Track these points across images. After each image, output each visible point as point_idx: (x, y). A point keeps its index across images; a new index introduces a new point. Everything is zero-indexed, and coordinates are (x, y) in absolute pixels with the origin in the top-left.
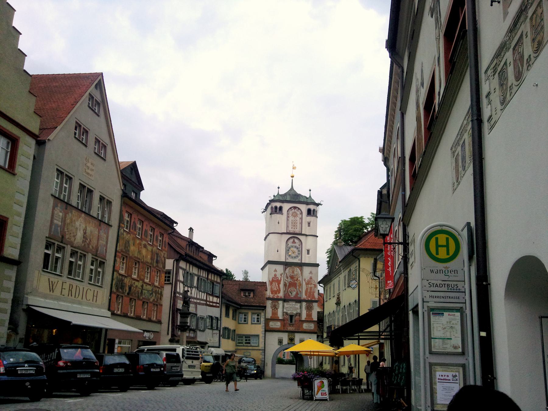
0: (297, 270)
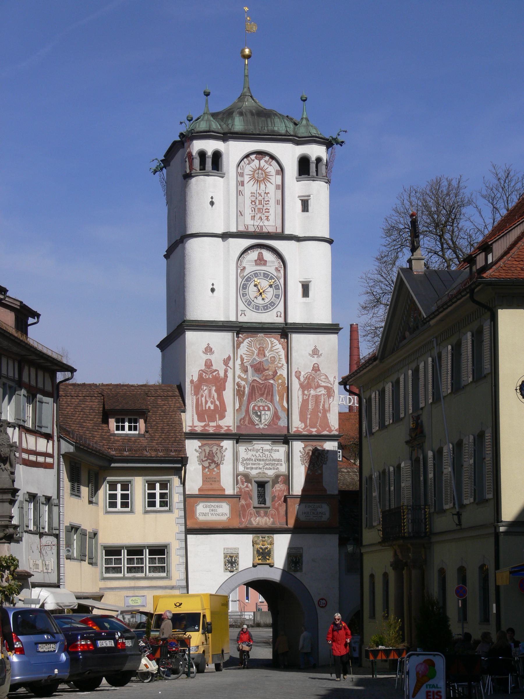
0: (274, 345)
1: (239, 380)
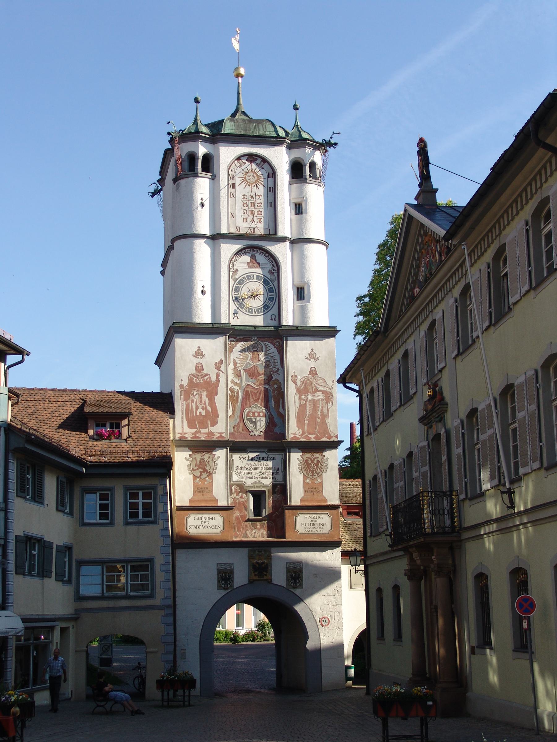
1: (233, 385)
